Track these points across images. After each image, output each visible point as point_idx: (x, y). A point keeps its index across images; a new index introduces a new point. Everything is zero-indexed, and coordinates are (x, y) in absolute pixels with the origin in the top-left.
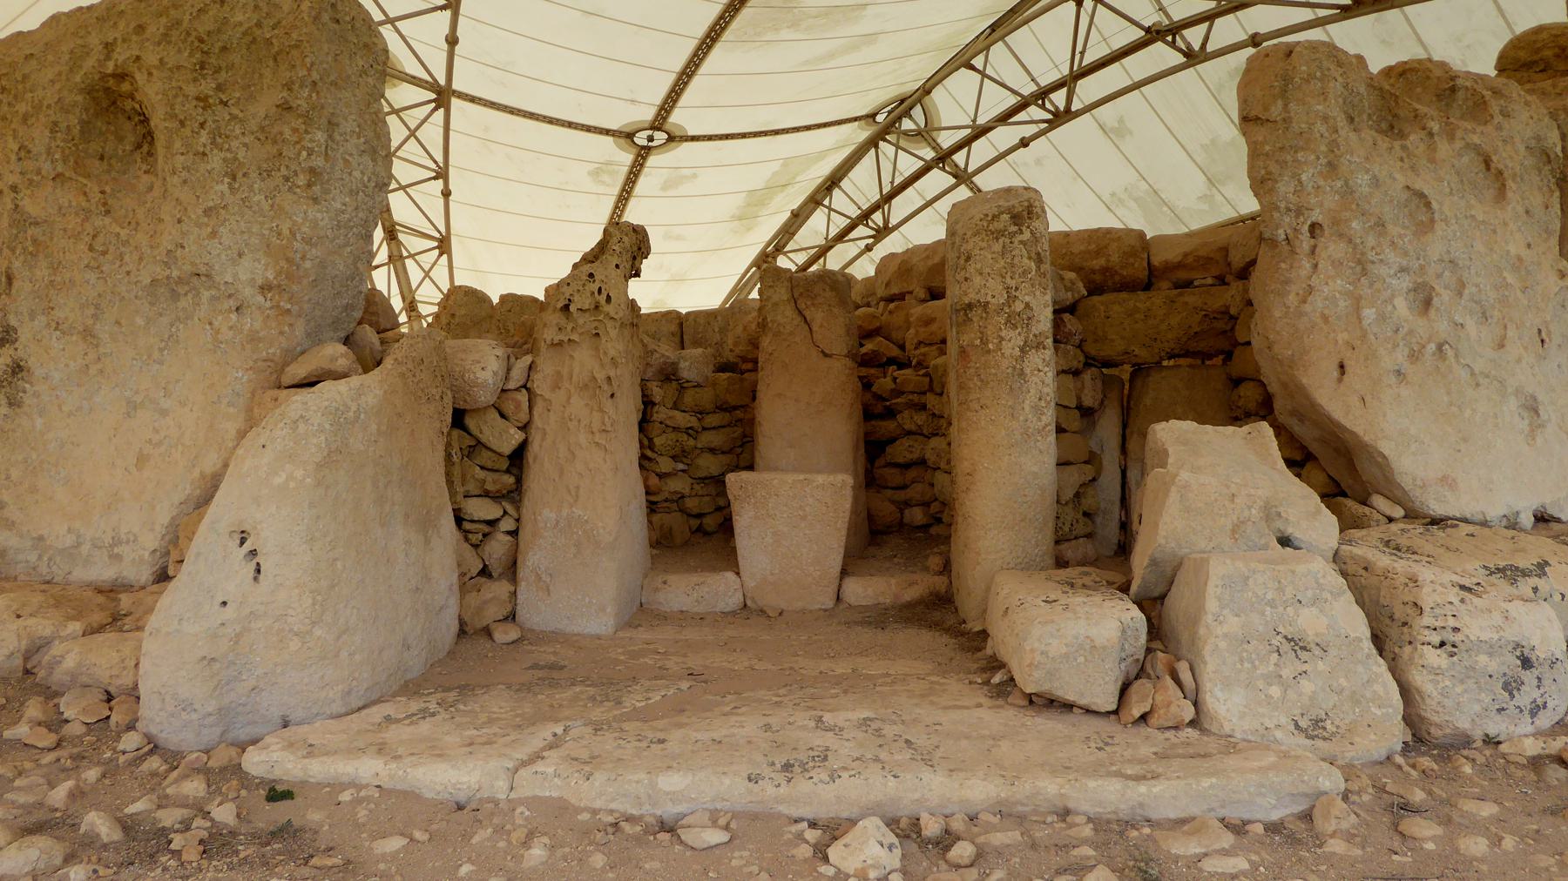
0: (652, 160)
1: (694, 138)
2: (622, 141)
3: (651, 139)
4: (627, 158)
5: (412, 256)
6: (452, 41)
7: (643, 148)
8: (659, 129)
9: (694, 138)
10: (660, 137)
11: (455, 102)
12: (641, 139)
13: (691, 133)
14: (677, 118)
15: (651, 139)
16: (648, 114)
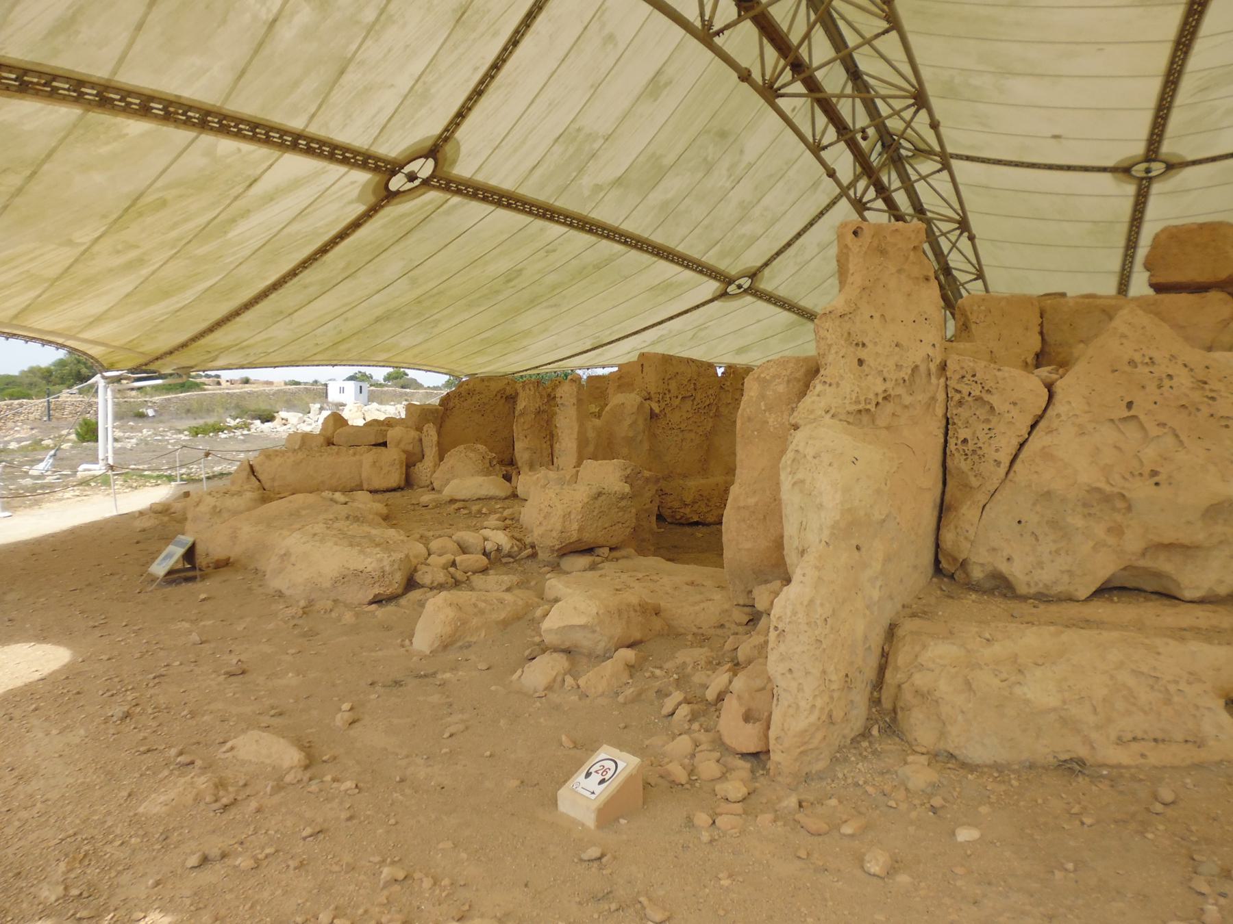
0: (1156, 188)
1: (1194, 163)
2: (1120, 175)
3: (1148, 171)
4: (1131, 189)
5: (962, 285)
6: (934, 126)
7: (1142, 179)
8: (1154, 160)
9: (1194, 163)
10: (1157, 168)
11: (955, 164)
12: (1139, 170)
13: (1190, 158)
14: (1166, 148)
15: (1148, 171)
16: (1139, 149)
